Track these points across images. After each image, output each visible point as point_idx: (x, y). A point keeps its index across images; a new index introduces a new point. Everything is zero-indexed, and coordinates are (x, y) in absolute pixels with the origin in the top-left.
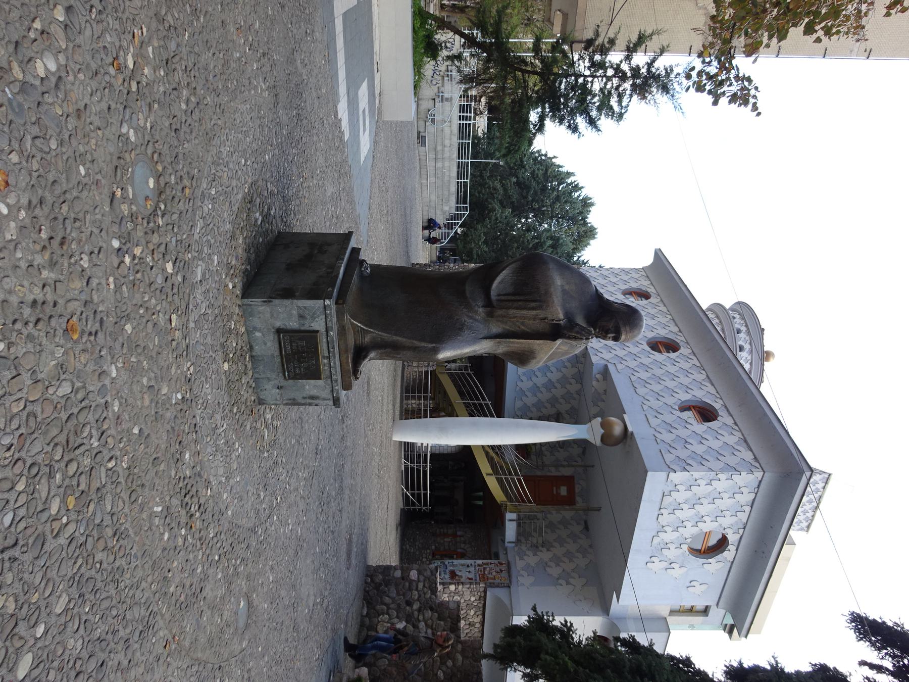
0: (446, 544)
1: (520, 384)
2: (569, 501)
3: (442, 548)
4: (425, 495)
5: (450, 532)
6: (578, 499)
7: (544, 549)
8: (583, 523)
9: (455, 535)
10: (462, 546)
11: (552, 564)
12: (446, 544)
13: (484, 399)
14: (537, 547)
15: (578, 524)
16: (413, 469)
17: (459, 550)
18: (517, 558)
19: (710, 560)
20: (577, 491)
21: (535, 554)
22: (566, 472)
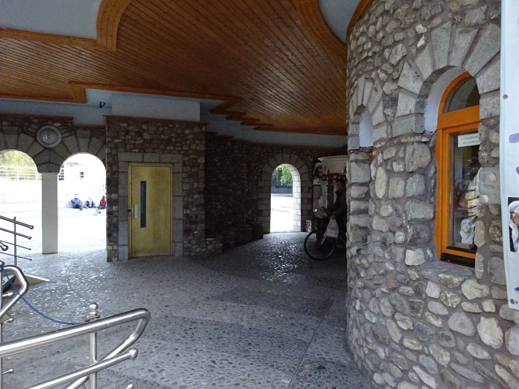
0: (398, 189)
3: (422, 212)
10: (406, 105)
12: (398, 189)
17: (431, 122)
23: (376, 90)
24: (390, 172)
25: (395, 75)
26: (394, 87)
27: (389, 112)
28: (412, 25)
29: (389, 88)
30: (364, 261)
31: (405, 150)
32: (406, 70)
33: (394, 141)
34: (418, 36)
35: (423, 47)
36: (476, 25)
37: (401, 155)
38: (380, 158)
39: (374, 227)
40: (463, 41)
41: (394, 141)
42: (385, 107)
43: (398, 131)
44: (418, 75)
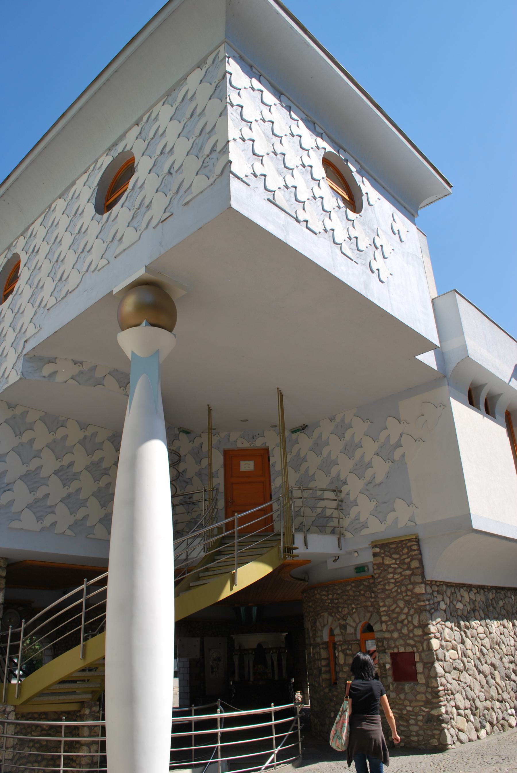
1: (59, 529)
2: (262, 456)
4: (279, 715)
5: (324, 654)
6: (259, 443)
7: (345, 489)
8: (294, 436)
9: (332, 646)
10: (350, 630)
11: (368, 474)
13: (79, 595)
14: (342, 501)
15: (297, 442)
16: (226, 751)
18: (365, 532)
19: (364, 193)
20: (246, 445)
21: (355, 503)
22: (218, 460)
23: (335, 621)
24: (346, 655)
25: (345, 618)
26: (344, 622)
27: (343, 631)
28: (351, 604)
29: (342, 622)
30: (335, 693)
31: (352, 646)
32: (349, 618)
33: (345, 642)
34: (353, 608)
35: (355, 612)
36: (371, 612)
37: (350, 647)
38: (340, 648)
39: (340, 676)
40: (368, 615)
41: (345, 642)
42: (341, 628)
43: (348, 639)
44: (354, 621)
